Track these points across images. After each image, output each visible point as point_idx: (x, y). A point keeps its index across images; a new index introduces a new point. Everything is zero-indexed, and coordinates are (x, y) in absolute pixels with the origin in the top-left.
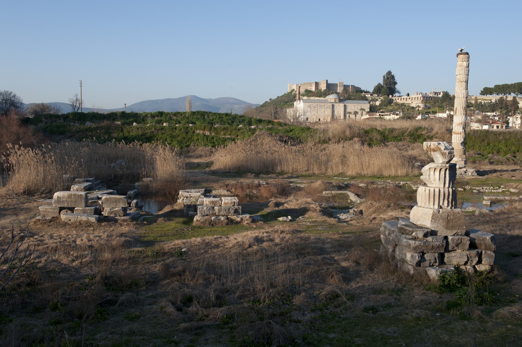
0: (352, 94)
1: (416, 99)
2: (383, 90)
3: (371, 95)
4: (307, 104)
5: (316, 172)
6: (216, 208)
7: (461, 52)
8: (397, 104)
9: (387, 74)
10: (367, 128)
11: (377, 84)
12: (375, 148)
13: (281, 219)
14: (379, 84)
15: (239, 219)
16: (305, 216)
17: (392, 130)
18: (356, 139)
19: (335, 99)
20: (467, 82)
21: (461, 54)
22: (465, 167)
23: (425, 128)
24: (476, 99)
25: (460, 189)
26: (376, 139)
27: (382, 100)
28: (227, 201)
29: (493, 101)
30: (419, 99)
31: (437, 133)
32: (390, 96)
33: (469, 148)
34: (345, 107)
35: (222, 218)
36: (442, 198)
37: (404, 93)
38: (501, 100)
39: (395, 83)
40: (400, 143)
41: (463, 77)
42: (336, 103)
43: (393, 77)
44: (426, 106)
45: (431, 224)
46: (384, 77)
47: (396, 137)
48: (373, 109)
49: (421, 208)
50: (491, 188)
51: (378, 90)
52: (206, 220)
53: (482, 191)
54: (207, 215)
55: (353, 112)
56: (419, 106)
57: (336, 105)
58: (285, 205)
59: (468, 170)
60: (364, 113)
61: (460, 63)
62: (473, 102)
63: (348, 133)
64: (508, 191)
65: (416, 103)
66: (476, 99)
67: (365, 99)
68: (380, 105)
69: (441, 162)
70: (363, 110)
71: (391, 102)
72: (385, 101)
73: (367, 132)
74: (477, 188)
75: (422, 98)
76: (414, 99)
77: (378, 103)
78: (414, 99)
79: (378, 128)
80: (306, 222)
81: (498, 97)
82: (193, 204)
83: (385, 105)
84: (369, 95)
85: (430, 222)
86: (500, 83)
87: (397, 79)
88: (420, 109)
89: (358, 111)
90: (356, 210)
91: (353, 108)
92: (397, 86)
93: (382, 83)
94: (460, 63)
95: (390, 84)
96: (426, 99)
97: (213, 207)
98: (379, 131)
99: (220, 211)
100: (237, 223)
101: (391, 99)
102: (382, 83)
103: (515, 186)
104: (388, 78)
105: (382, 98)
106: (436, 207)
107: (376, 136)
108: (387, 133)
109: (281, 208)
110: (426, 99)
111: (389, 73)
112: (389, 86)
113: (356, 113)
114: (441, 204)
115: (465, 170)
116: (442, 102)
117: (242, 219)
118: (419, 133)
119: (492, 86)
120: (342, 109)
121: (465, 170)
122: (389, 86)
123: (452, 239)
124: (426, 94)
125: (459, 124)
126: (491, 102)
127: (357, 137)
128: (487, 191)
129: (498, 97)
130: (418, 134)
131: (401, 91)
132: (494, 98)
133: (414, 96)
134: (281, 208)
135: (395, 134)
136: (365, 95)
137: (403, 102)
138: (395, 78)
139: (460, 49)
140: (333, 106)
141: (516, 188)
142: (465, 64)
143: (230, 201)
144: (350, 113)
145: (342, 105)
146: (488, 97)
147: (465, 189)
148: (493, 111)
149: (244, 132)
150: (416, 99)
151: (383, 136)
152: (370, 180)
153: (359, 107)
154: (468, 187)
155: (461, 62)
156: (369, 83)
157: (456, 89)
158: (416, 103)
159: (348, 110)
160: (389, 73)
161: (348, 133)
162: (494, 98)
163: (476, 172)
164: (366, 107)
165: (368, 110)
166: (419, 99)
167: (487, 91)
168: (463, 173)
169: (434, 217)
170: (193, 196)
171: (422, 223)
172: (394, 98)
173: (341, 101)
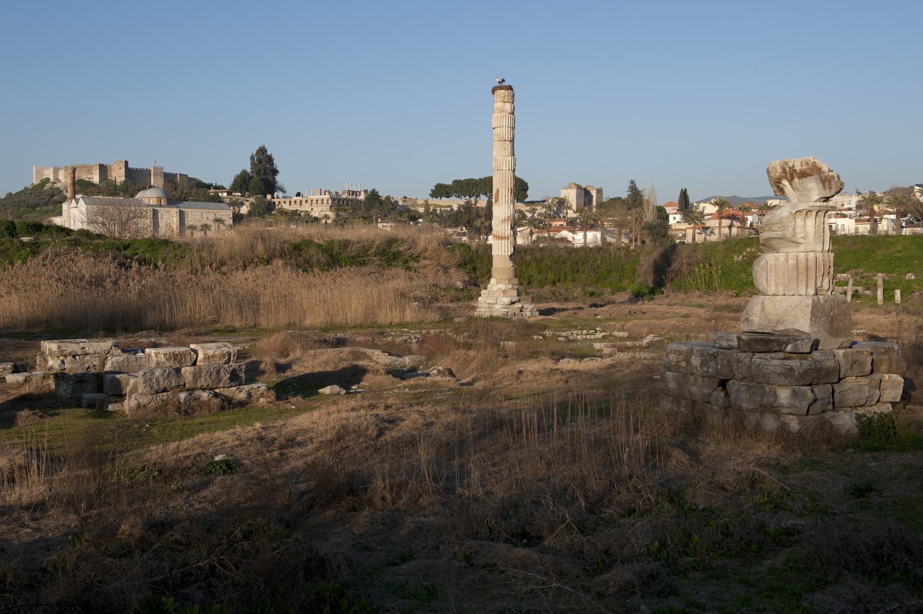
1: (320, 202)
2: (252, 185)
3: (229, 193)
5: (237, 324)
6: (187, 371)
7: (502, 86)
8: (283, 212)
9: (258, 152)
10: (298, 240)
11: (239, 173)
13: (327, 390)
14: (244, 172)
15: (242, 396)
16: (362, 383)
18: (279, 262)
19: (159, 199)
20: (512, 141)
21: (501, 88)
22: (519, 301)
23: (403, 241)
24: (427, 205)
26: (318, 262)
27: (252, 204)
28: (211, 352)
29: (455, 208)
30: (325, 202)
31: (426, 250)
32: (269, 197)
33: (483, 276)
34: (182, 215)
35: (205, 395)
36: (819, 274)
37: (291, 192)
38: (468, 207)
39: (275, 172)
40: (363, 269)
41: (505, 133)
42: (161, 206)
43: (270, 159)
44: (338, 215)
45: (812, 326)
46: (252, 158)
47: (353, 257)
49: (779, 298)
50: (585, 332)
51: (243, 183)
52: (165, 403)
53: (571, 338)
54: (165, 390)
55: (199, 224)
56: (326, 217)
57: (161, 211)
58: (295, 367)
59: (526, 306)
61: (500, 104)
62: (421, 210)
63: (260, 248)
64: (611, 335)
65: (321, 210)
66: (427, 205)
67: (217, 199)
68: (250, 214)
69: (816, 197)
70: (218, 221)
71: (270, 207)
74: (563, 334)
75: (330, 201)
76: (314, 202)
77: (244, 210)
78: (314, 202)
79: (316, 240)
80: (399, 388)
81: (462, 201)
82: (92, 370)
83: (260, 215)
84: (225, 194)
85: (809, 322)
86: (462, 177)
87: (278, 163)
88: (329, 221)
89: (209, 223)
90: (441, 368)
91: (198, 217)
92: (278, 178)
93: (249, 170)
94: (499, 105)
95: (265, 173)
96: (338, 203)
97: (178, 370)
98: (320, 246)
99: (196, 376)
100: (242, 404)
101: (270, 202)
102: (249, 170)
103: (619, 325)
104: (260, 161)
105: (252, 199)
106: (811, 291)
107: (314, 254)
108: (336, 249)
109: (289, 374)
110: (338, 203)
111: (262, 151)
112: (261, 178)
113: (205, 227)
114: (819, 285)
115: (520, 305)
116: (368, 209)
117: (249, 395)
118: (394, 249)
119: (449, 182)
120: (175, 220)
121: (520, 305)
122: (261, 178)
123: (844, 354)
125: (503, 221)
126: (452, 210)
127: (281, 257)
128: (579, 337)
129: (462, 201)
130: (392, 250)
131: (286, 188)
132: (455, 203)
133: (315, 197)
134: (289, 374)
135: (353, 250)
136: (217, 194)
137: (293, 207)
138: (275, 162)
139: (498, 80)
140: (155, 213)
141: (622, 329)
142: (508, 107)
143: (218, 352)
144: (193, 228)
145: (174, 211)
146: (444, 201)
147: (544, 336)
148: (456, 226)
149: (7, 250)
150: (320, 202)
151: (331, 256)
153: (212, 217)
154: (547, 333)
155: (500, 102)
156: (222, 171)
158: (321, 210)
159: (189, 221)
160: (262, 151)
161: (260, 248)
162: (455, 203)
164: (227, 215)
165: (231, 222)
166: (325, 202)
167: (441, 191)
168: (518, 312)
169: (816, 311)
170: (91, 351)
171: (790, 327)
172: (276, 201)
173: (171, 202)
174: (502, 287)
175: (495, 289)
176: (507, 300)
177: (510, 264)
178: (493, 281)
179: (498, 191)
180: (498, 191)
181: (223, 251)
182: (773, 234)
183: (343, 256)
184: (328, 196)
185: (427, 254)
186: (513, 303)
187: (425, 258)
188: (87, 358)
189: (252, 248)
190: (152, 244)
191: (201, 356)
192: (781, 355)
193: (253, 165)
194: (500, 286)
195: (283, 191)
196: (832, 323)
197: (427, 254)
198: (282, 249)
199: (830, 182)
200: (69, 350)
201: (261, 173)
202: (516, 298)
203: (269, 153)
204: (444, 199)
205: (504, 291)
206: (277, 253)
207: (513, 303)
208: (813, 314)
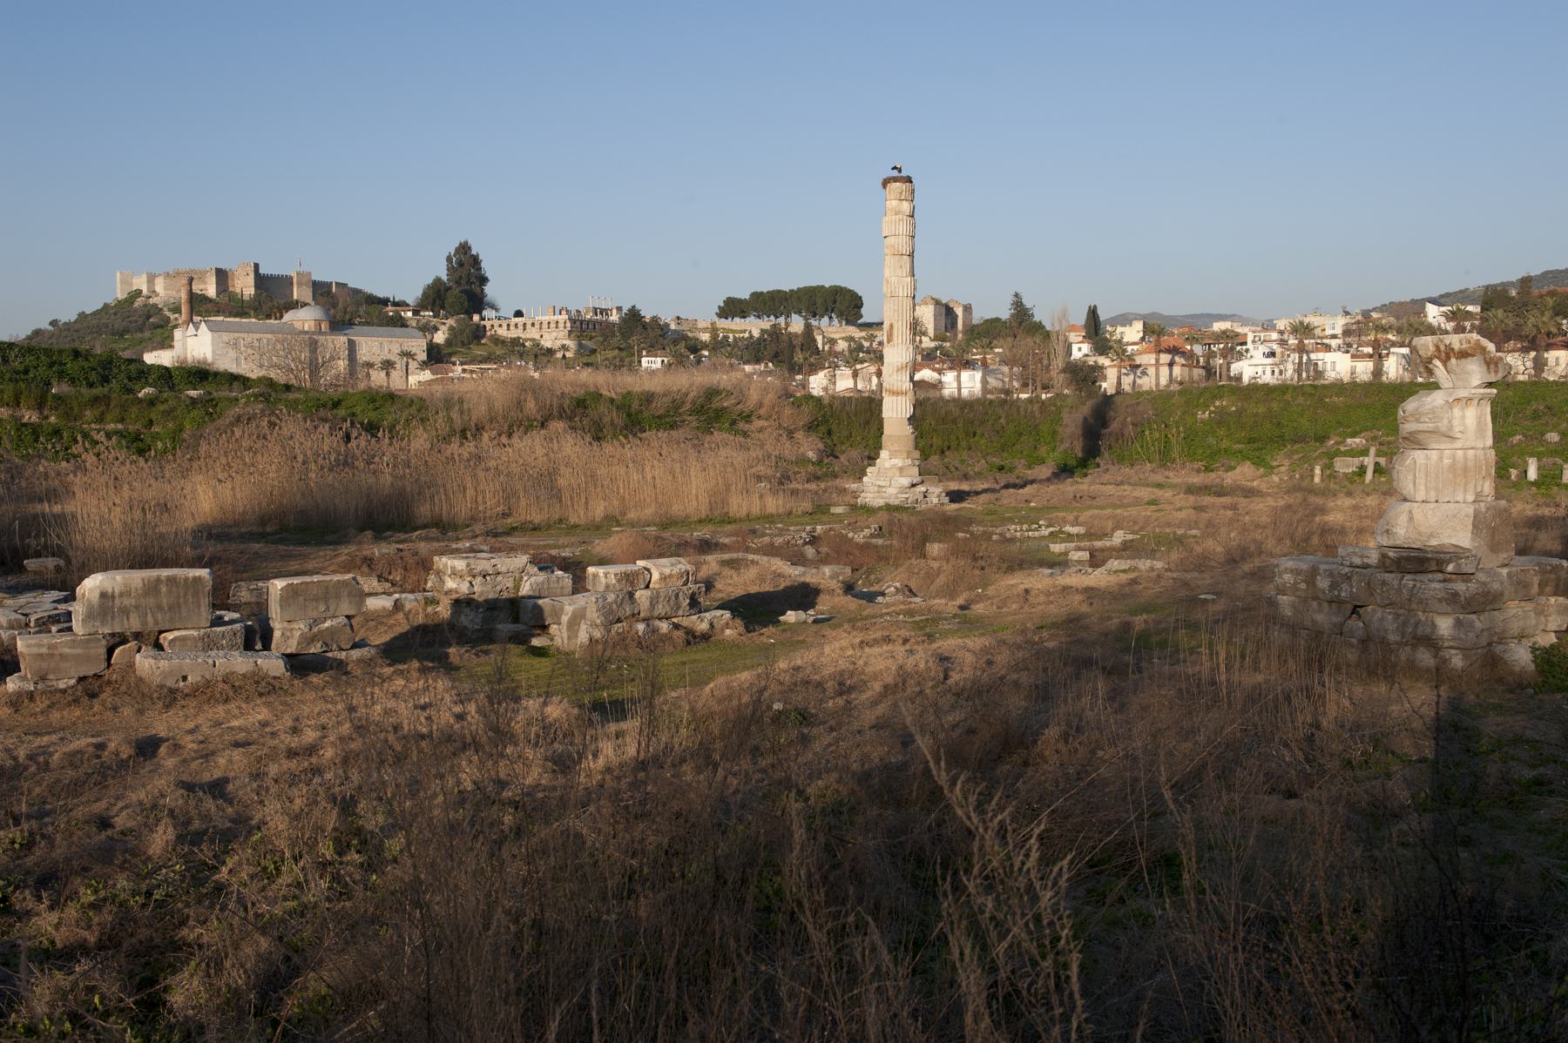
0: (351, 309)
1: (553, 325)
2: (450, 299)
3: (416, 313)
4: (226, 337)
6: (642, 595)
8: (497, 341)
9: (457, 250)
10: (581, 393)
11: (430, 281)
12: (608, 448)
14: (438, 281)
15: (704, 626)
17: (648, 398)
18: (558, 426)
19: (318, 322)
20: (911, 255)
21: (895, 180)
24: (714, 330)
25: (961, 535)
27: (451, 329)
28: (667, 571)
29: (756, 334)
30: (561, 325)
31: (761, 405)
32: (476, 318)
35: (664, 626)
37: (507, 311)
38: (775, 333)
39: (483, 280)
40: (674, 433)
41: (903, 244)
42: (320, 332)
43: (476, 261)
44: (580, 345)
46: (449, 259)
48: (436, 356)
50: (1025, 527)
51: (435, 297)
52: (622, 637)
54: (619, 621)
56: (564, 347)
59: (931, 489)
60: (413, 365)
61: (895, 203)
62: (705, 337)
63: (531, 406)
64: (1061, 532)
65: (555, 338)
66: (714, 330)
67: (400, 322)
68: (448, 342)
69: (1477, 383)
70: (408, 355)
71: (479, 333)
72: (462, 331)
73: (581, 403)
76: (545, 326)
77: (440, 338)
78: (545, 326)
81: (766, 323)
82: (505, 595)
83: (463, 344)
84: (410, 314)
86: (765, 288)
87: (487, 267)
88: (568, 355)
91: (376, 350)
92: (488, 289)
93: (445, 278)
94: (892, 204)
95: (469, 283)
96: (580, 327)
97: (631, 595)
98: (612, 400)
99: (654, 601)
100: (705, 637)
101: (478, 325)
102: (445, 278)
103: (1071, 517)
104: (461, 264)
105: (451, 322)
108: (635, 405)
110: (580, 327)
111: (464, 248)
112: (463, 287)
113: (388, 365)
116: (625, 336)
117: (712, 625)
118: (716, 404)
119: (744, 295)
121: (923, 489)
122: (463, 287)
126: (751, 336)
127: (560, 417)
129: (766, 323)
131: (500, 303)
132: (754, 326)
133: (546, 318)
135: (659, 406)
136: (397, 313)
137: (513, 334)
138: (483, 265)
141: (1076, 523)
142: (906, 206)
143: (676, 570)
144: (370, 365)
146: (737, 324)
147: (972, 533)
148: (758, 361)
149: (173, 410)
150: (553, 325)
151: (629, 415)
152: (745, 527)
153: (396, 349)
154: (974, 528)
155: (894, 199)
156: (405, 276)
157: (887, 273)
158: (555, 338)
160: (464, 248)
161: (531, 406)
162: (754, 326)
163: (947, 494)
164: (418, 346)
165: (423, 356)
166: (561, 325)
167: (732, 308)
168: (920, 498)
169: (1478, 523)
170: (504, 569)
171: (1446, 541)
172: (487, 324)
174: (898, 462)
175: (887, 465)
176: (905, 482)
177: (909, 429)
178: (884, 454)
179: (891, 326)
180: (891, 326)
181: (480, 411)
182: (1421, 427)
183: (646, 414)
184: (565, 316)
185: (762, 412)
186: (913, 485)
187: (759, 417)
188: (500, 578)
189: (519, 405)
190: (373, 400)
191: (656, 576)
192: (1440, 576)
193: (450, 269)
194: (895, 461)
195: (493, 307)
196: (1493, 535)
197: (762, 412)
198: (561, 407)
199: (1496, 365)
200: (479, 569)
202: (918, 479)
204: (737, 320)
205: (901, 469)
206: (555, 412)
207: (913, 485)
208: (1475, 526)
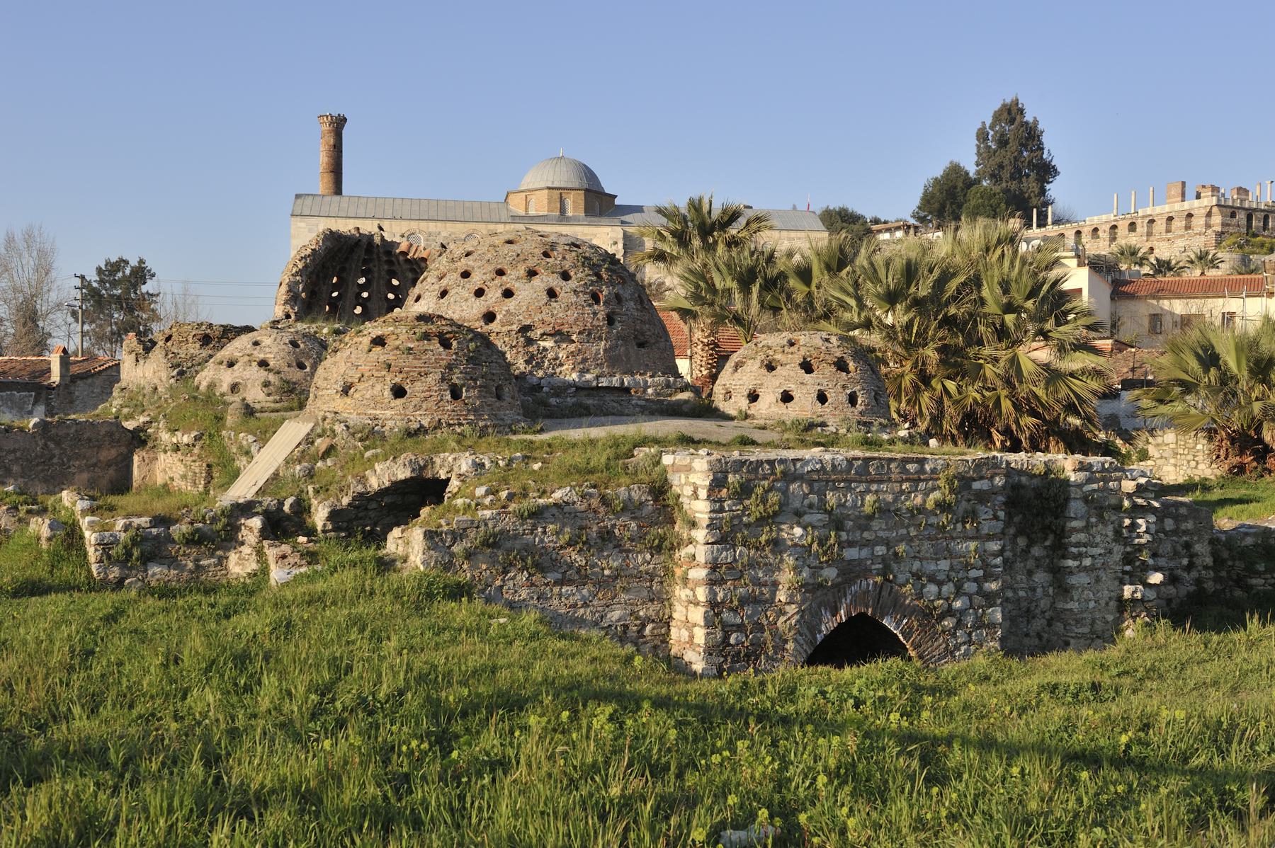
1: (1178, 224)
9: (997, 117)
11: (938, 173)
14: (955, 171)
30: (1198, 222)
43: (1031, 136)
46: (982, 135)
75: (1217, 219)
76: (1160, 226)
87: (1055, 147)
92: (1054, 189)
95: (1017, 175)
104: (1003, 142)
111: (1011, 112)
124: (1242, 191)
138: (1046, 140)
150: (1178, 224)
160: (1011, 112)
166: (1198, 222)
193: (984, 154)
201: (1006, 174)
203: (1029, 118)
